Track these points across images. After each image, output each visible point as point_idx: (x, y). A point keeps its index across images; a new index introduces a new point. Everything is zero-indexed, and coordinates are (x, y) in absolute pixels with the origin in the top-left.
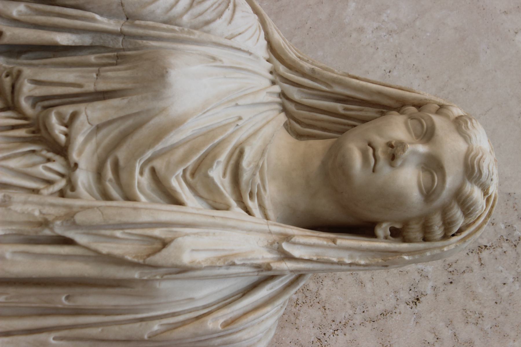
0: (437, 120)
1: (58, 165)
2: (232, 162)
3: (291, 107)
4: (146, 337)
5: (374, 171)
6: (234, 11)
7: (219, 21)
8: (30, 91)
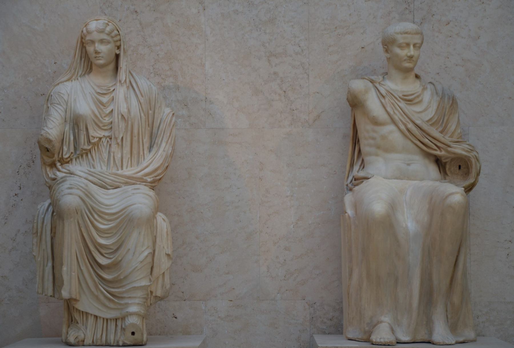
0: (88, 38)
1: (104, 140)
2: (101, 95)
3: (83, 73)
4: (145, 117)
5: (102, 57)
6: (61, 93)
7: (64, 98)
8: (86, 146)
